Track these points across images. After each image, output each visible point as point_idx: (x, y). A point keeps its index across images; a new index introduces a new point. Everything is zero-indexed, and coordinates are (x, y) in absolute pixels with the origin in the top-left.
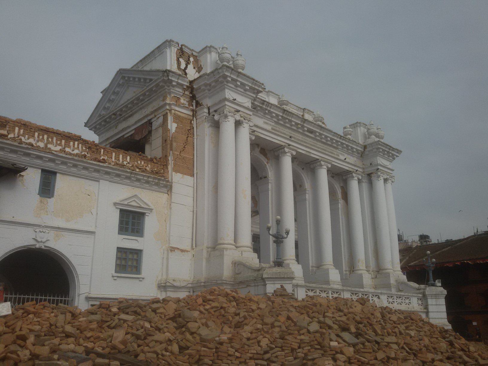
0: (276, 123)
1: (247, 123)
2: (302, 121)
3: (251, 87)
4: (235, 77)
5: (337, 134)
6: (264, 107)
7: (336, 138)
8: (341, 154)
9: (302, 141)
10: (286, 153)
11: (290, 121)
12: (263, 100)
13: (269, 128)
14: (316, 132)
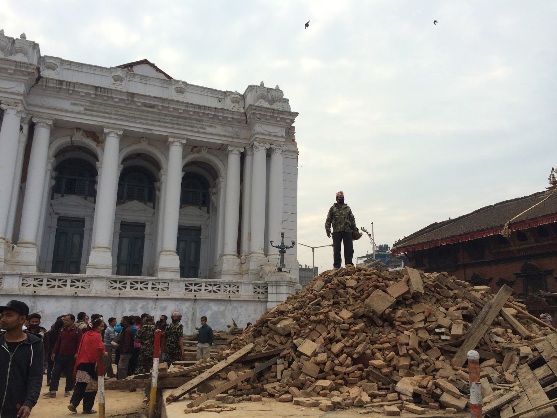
1: (12, 109)
2: (128, 96)
5: (192, 104)
6: (64, 87)
7: (191, 109)
8: (208, 126)
9: (138, 118)
10: (109, 133)
12: (59, 81)
14: (158, 106)
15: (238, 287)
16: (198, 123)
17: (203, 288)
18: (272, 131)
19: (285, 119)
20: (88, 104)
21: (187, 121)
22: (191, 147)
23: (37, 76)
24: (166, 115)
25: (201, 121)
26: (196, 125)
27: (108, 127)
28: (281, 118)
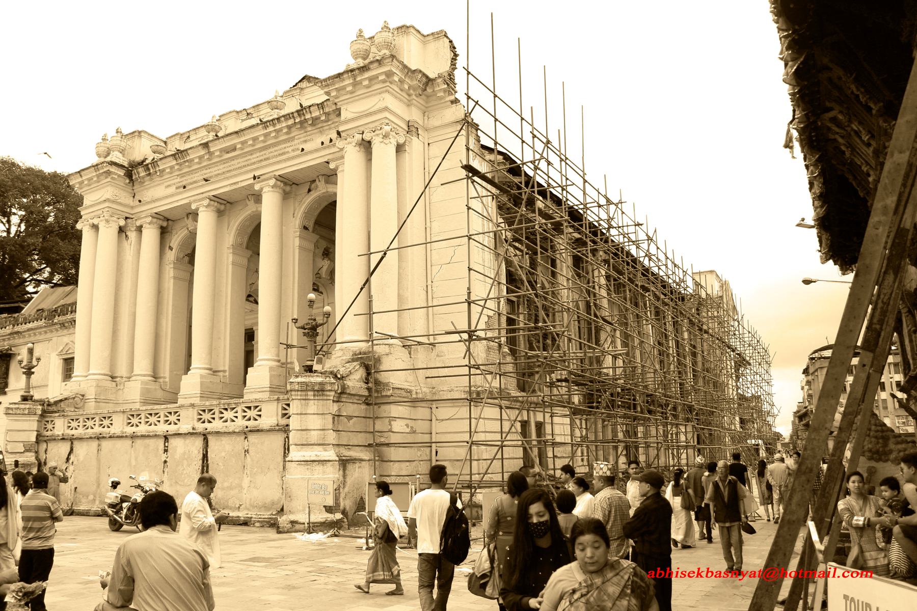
0: (182, 176)
3: (98, 176)
4: (80, 179)
10: (197, 209)
11: (192, 160)
13: (172, 190)
15: (260, 411)
16: (288, 144)
17: (217, 416)
18: (362, 109)
19: (376, 77)
20: (178, 180)
21: (276, 148)
22: (290, 185)
23: (121, 172)
24: (251, 153)
25: (293, 139)
26: (286, 150)
27: (195, 201)
28: (370, 79)
